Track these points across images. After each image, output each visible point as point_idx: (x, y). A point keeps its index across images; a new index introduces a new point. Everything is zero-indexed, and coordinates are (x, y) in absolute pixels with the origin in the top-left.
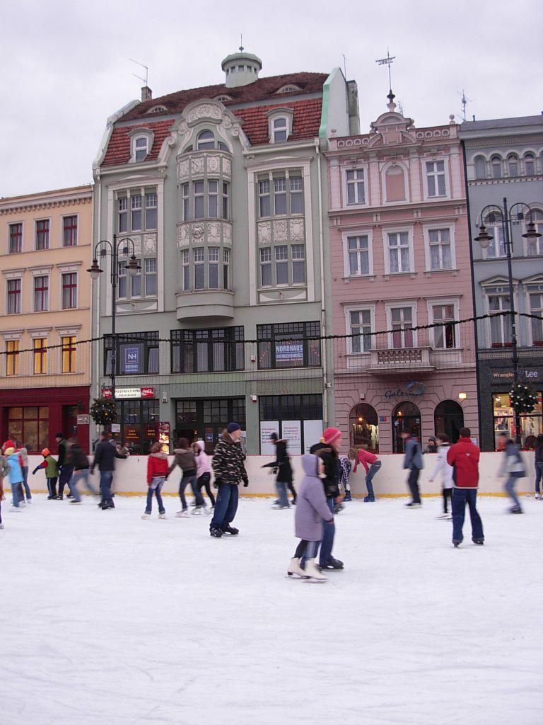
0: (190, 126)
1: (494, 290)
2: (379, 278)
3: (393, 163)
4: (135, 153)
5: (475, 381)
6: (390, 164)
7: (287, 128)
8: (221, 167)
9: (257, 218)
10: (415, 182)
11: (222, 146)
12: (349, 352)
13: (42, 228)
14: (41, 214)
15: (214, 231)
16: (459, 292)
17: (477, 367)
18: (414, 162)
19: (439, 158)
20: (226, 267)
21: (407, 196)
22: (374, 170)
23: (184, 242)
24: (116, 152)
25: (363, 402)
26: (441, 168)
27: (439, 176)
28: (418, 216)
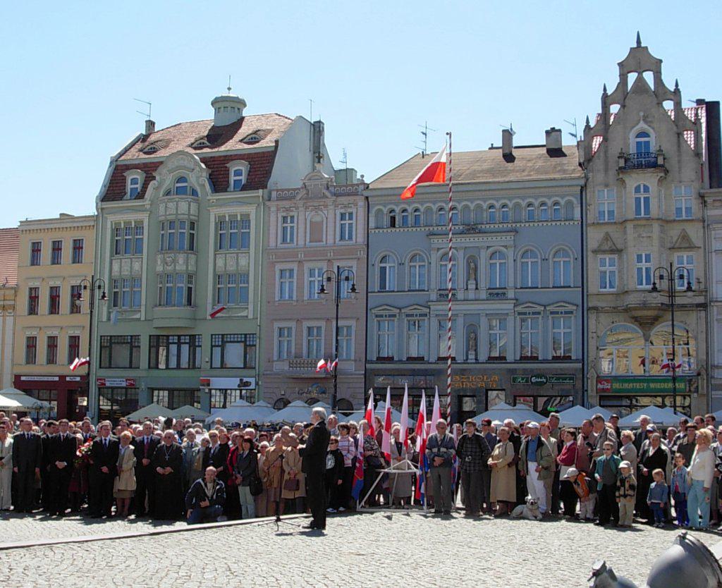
0: (170, 172)
4: (129, 190)
6: (313, 213)
7: (243, 178)
8: (189, 208)
9: (215, 251)
11: (194, 193)
12: (275, 359)
13: (57, 248)
14: (56, 236)
15: (181, 261)
20: (190, 289)
21: (324, 240)
22: (301, 218)
23: (159, 268)
24: (114, 189)
25: (283, 397)
27: (349, 224)
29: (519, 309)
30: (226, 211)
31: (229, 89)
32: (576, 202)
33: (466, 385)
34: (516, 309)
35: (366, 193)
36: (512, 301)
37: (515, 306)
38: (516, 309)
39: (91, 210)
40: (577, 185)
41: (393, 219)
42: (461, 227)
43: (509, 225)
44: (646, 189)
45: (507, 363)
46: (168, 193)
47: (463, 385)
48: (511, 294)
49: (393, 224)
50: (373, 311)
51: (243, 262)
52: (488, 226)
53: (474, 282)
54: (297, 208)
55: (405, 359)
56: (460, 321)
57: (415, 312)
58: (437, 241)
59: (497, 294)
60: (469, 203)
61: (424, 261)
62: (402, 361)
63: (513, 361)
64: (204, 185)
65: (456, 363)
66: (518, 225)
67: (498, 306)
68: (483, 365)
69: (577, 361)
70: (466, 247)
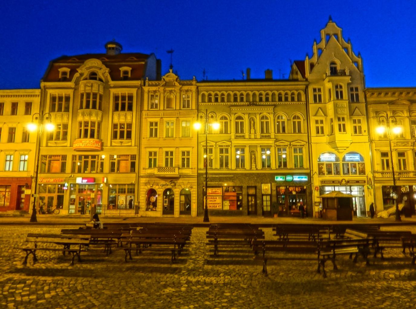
0: (87, 69)
2: (161, 139)
5: (196, 181)
11: (101, 80)
16: (193, 146)
17: (197, 176)
29: (277, 143)
30: (120, 92)
32: (302, 93)
37: (275, 142)
40: (302, 85)
44: (341, 87)
50: (201, 143)
51: (129, 118)
56: (247, 150)
57: (224, 144)
62: (217, 169)
69: (307, 169)
70: (249, 113)
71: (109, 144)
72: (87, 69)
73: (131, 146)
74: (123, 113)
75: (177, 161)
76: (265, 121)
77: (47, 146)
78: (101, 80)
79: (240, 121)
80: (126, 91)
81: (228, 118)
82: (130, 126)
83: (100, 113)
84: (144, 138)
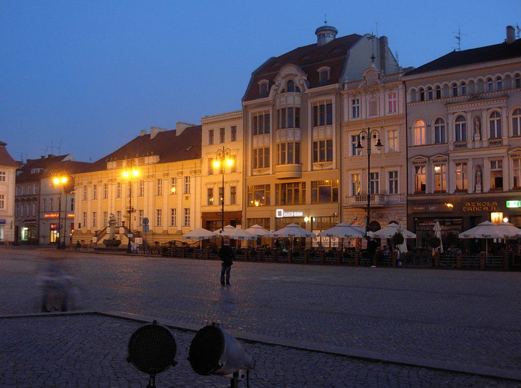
0: (283, 78)
1: (417, 163)
3: (372, 95)
8: (294, 101)
10: (382, 105)
11: (298, 90)
12: (350, 195)
14: (222, 125)
15: (290, 135)
18: (382, 94)
19: (393, 92)
21: (378, 113)
24: (254, 91)
26: (394, 97)
28: (383, 124)
29: (510, 152)
31: (326, 22)
33: (475, 209)
34: (509, 153)
35: (404, 79)
36: (505, 147)
37: (508, 151)
38: (509, 153)
39: (238, 106)
41: (422, 95)
42: (468, 97)
43: (503, 92)
45: (503, 192)
46: (283, 91)
47: (472, 209)
48: (505, 142)
49: (422, 99)
51: (329, 133)
52: (487, 94)
53: (479, 135)
54: (360, 94)
55: (433, 192)
56: (470, 164)
58: (453, 109)
59: (495, 143)
60: (473, 79)
61: (444, 123)
62: (431, 193)
63: (508, 190)
64: (303, 84)
65: (468, 194)
66: (509, 91)
67: (497, 151)
68: (486, 194)
70: (473, 111)
71: (309, 169)
72: (283, 78)
73: (332, 169)
74: (322, 128)
75: (384, 183)
76: (495, 119)
77: (252, 175)
78: (298, 90)
79: (461, 123)
80: (324, 99)
81: (445, 121)
82: (330, 143)
83: (298, 132)
84: (345, 158)
